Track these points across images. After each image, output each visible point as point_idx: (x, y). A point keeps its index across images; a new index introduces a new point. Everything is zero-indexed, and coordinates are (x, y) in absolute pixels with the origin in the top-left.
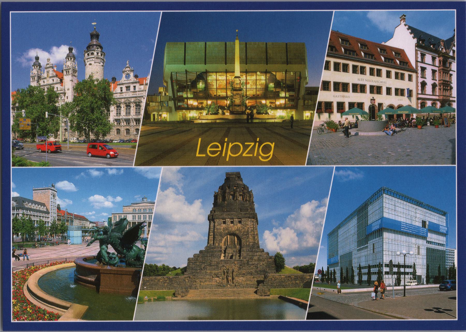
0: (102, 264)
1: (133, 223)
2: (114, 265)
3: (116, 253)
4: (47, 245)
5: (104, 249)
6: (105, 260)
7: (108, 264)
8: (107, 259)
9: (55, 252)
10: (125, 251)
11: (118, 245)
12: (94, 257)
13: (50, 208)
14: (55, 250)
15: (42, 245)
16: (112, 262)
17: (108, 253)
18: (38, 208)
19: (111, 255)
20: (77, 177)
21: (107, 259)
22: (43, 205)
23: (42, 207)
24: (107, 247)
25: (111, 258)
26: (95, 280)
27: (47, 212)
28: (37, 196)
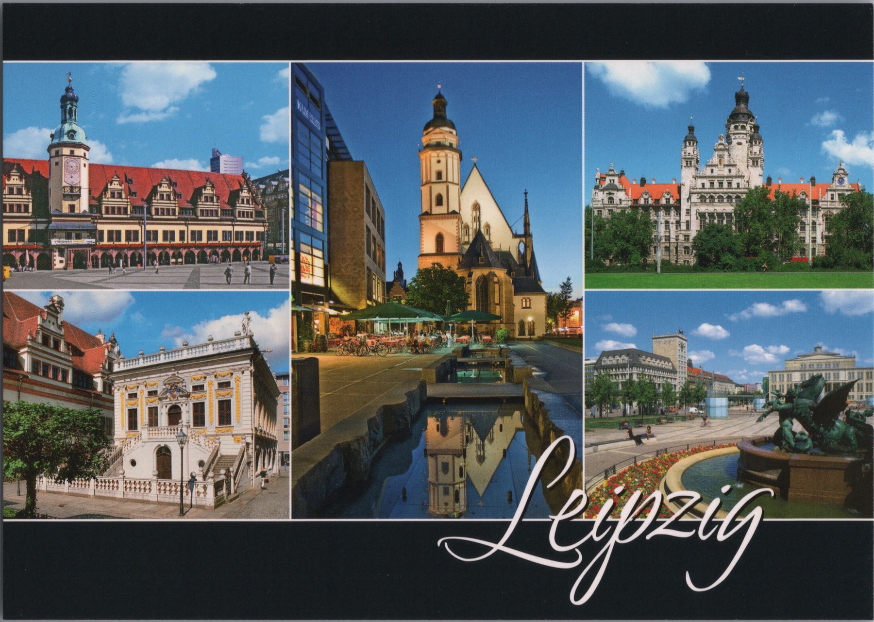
0: (783, 451)
2: (805, 452)
3: (807, 433)
4: (677, 419)
5: (787, 426)
6: (788, 443)
8: (793, 443)
9: (690, 430)
11: (810, 419)
12: (769, 438)
13: (676, 364)
14: (690, 427)
15: (670, 420)
16: (801, 447)
17: (794, 433)
18: (660, 365)
19: (798, 436)
20: (733, 318)
21: (793, 443)
24: (792, 423)
25: (797, 440)
27: (674, 371)
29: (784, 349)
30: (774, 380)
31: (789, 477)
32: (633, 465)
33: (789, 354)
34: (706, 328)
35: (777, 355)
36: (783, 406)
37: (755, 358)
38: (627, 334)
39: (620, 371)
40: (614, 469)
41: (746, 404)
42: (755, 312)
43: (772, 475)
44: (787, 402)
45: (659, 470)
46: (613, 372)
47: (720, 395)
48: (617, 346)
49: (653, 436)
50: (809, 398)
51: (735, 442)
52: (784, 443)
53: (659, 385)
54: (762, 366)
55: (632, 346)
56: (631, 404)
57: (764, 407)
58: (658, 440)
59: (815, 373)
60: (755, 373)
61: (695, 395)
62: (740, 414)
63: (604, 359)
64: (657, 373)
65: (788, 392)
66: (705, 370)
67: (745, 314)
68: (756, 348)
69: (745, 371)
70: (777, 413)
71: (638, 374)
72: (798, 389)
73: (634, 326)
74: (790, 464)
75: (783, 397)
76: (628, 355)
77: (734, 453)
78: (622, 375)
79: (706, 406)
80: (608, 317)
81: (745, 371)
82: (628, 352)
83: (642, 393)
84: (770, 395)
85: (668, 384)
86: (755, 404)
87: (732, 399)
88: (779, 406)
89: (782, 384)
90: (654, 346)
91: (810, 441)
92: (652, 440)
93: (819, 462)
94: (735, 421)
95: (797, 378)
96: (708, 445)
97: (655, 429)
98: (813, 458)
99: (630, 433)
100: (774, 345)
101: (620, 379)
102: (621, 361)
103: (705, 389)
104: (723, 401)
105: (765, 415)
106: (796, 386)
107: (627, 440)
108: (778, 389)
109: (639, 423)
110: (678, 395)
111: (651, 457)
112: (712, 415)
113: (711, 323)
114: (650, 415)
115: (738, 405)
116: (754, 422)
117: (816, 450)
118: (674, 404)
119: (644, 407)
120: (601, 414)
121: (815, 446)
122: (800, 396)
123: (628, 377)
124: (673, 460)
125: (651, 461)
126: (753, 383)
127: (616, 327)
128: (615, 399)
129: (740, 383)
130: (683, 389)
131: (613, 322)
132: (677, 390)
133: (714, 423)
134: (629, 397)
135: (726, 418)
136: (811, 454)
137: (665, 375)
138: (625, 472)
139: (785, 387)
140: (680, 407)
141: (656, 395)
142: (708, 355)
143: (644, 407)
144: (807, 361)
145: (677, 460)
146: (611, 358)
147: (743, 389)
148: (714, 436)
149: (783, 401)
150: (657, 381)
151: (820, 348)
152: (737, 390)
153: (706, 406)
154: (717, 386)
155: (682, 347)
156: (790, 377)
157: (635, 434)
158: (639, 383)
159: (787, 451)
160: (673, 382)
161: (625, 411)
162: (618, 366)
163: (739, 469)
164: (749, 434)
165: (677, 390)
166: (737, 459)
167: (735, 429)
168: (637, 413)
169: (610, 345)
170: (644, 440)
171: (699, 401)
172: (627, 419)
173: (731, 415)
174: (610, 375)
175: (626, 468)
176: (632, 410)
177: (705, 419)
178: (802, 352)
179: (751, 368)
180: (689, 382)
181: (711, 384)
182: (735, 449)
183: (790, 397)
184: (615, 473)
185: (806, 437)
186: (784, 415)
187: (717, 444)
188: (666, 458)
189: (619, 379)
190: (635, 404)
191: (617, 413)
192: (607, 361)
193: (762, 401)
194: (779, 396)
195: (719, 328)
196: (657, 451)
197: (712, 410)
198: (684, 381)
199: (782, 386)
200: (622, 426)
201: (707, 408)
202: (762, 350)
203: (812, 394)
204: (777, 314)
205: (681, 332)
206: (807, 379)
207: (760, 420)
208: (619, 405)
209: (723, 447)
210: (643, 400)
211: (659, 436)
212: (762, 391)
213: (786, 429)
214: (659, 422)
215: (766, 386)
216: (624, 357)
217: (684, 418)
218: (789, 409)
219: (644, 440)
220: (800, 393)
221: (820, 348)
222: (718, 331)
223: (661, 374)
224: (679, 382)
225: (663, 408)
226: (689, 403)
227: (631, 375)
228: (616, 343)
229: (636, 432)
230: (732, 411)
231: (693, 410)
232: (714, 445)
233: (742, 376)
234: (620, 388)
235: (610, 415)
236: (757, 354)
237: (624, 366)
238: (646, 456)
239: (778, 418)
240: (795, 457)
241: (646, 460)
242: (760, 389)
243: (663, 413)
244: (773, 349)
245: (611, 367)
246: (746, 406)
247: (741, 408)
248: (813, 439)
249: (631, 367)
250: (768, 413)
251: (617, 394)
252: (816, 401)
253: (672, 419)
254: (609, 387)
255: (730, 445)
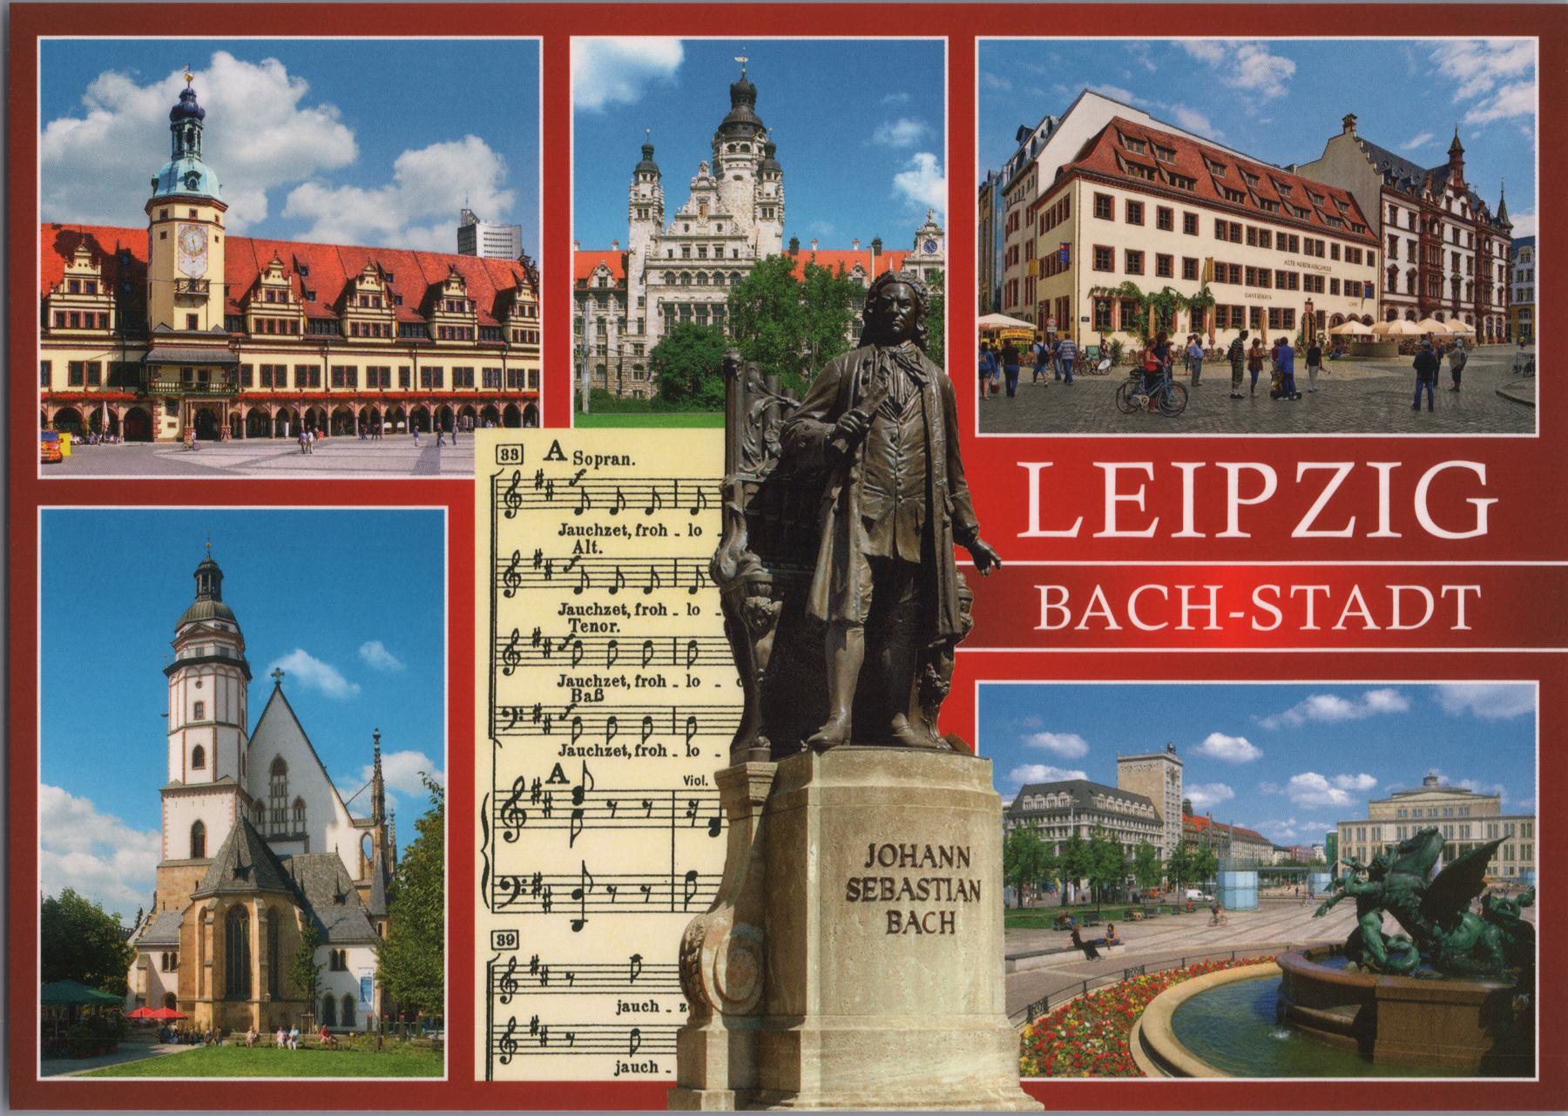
0: (1365, 969)
1: (1461, 847)
2: (1405, 972)
3: (1408, 936)
4: (1163, 912)
5: (1371, 924)
6: (1374, 955)
7: (1388, 970)
8: (1383, 956)
9: (1188, 933)
10: (1437, 930)
11: (1415, 912)
12: (1338, 946)
13: (1163, 810)
14: (1187, 926)
15: (1150, 913)
16: (1399, 963)
17: (1385, 938)
18: (1132, 811)
19: (1392, 942)
20: (1269, 724)
21: (1383, 956)
22: (1145, 801)
23: (1144, 807)
24: (1381, 919)
25: (1391, 951)
26: (1357, 1019)
27: (1158, 822)
28: (1129, 778)
29: (1366, 781)
30: (1348, 839)
31: (1375, 1019)
32: (1080, 997)
33: (1372, 790)
34: (1218, 743)
35: (1353, 793)
36: (1364, 887)
37: (1311, 797)
38: (1071, 754)
39: (1057, 822)
40: (1044, 1004)
41: (1295, 882)
42: (1312, 712)
43: (1344, 1016)
44: (1371, 879)
45: (1129, 1005)
46: (1044, 823)
47: (1245, 866)
48: (1052, 774)
49: (1117, 943)
50: (1412, 873)
51: (1274, 953)
52: (1366, 955)
53: (1130, 847)
54: (1324, 812)
55: (1080, 775)
56: (1077, 884)
57: (1328, 889)
58: (1128, 950)
59: (1425, 826)
60: (1312, 826)
61: (1198, 865)
62: (1282, 902)
63: (1027, 799)
64: (1125, 826)
65: (1374, 861)
66: (1215, 819)
67: (1292, 716)
68: (1313, 779)
69: (1292, 822)
70: (1353, 900)
71: (1090, 827)
72: (1393, 855)
73: (1082, 737)
74: (1378, 994)
75: (1364, 869)
76: (1071, 792)
77: (1271, 974)
78: (1060, 829)
79: (1218, 888)
80: (1032, 721)
81: (1292, 822)
82: (1071, 787)
83: (1098, 862)
84: (1341, 867)
85: (1147, 847)
86: (1312, 883)
87: (1266, 873)
88: (1356, 888)
89: (1365, 847)
90: (1122, 775)
91: (1414, 953)
92: (1116, 950)
93: (1433, 992)
94: (1274, 915)
95: (1390, 835)
96: (1221, 958)
97: (1121, 929)
98: (1418, 984)
99: (1076, 937)
100: (1347, 773)
101: (1057, 837)
102: (1058, 804)
103: (1216, 854)
104: (1248, 879)
105: (1330, 905)
106: (1388, 849)
107: (1069, 949)
108: (1354, 854)
109: (1092, 919)
110: (1164, 867)
111: (1113, 982)
112: (1228, 903)
113: (1228, 732)
114: (1112, 903)
115: (1278, 885)
116: (1310, 917)
117: (1426, 971)
118: (1158, 883)
119: (1100, 887)
120: (1020, 902)
121: (1424, 962)
122: (1396, 869)
123: (1071, 833)
124: (1155, 988)
125: (1114, 990)
126: (1308, 843)
127: (1049, 740)
128: (1047, 874)
129: (1280, 844)
130: (1175, 856)
131: (1041, 731)
132: (1164, 857)
133: (1232, 919)
134: (1073, 871)
135: (1254, 910)
136: (1418, 976)
137: (1141, 828)
138: (1065, 1010)
139: (1369, 850)
140: (1170, 889)
141: (1124, 867)
142: (1225, 791)
143: (1100, 887)
144: (1409, 804)
145: (1164, 987)
146: (1039, 798)
147: (1288, 856)
148: (1229, 943)
149: (1364, 877)
150: (1125, 840)
151: (1434, 779)
152: (1276, 858)
153: (1218, 888)
154: (1239, 851)
155: (1173, 776)
156: (1377, 834)
157: (1084, 939)
158: (1092, 844)
159: (1372, 971)
160: (1157, 843)
161: (1065, 895)
162: (1053, 813)
163: (1280, 1005)
164: (1301, 939)
165: (1164, 857)
166: (1276, 986)
167: (1274, 929)
168: (1089, 901)
169: (1038, 773)
170: (1102, 951)
171: (1204, 875)
172: (1070, 911)
173: (1264, 903)
174: (1037, 829)
175: (1069, 1002)
176: (1079, 895)
177: (1215, 912)
178: (1400, 786)
179: (1303, 815)
180: (1186, 843)
181: (1227, 846)
182: (1272, 967)
183: (1377, 870)
184: (1046, 1011)
185: (1406, 945)
186: (1366, 903)
187: (1239, 957)
188: (1141, 985)
189: (1054, 837)
190: (1084, 883)
191: (1052, 899)
192: (1031, 803)
193: (1325, 878)
194: (1356, 869)
195: (1242, 741)
196: (1126, 971)
197: (1228, 894)
198: (1177, 841)
199: (1362, 850)
200: (1060, 924)
201: (1220, 890)
202: (1325, 783)
203: (1418, 864)
204: (1352, 716)
205: (1170, 750)
206: (1410, 836)
207: (1320, 913)
208: (1055, 885)
209: (1249, 963)
210: (1100, 875)
211: (1129, 943)
212: (1324, 859)
213: (1370, 931)
214: (1129, 917)
215: (1331, 850)
216: (1063, 795)
217: (1176, 910)
218: (1375, 893)
219: (1102, 951)
220: (1395, 865)
221: (1434, 779)
222: (1240, 746)
223: (1133, 827)
224: (1166, 843)
225: (1137, 890)
226: (1185, 881)
227: (1077, 829)
228: (1049, 770)
229: (1087, 934)
230: (1268, 897)
231: (1193, 894)
232: (1232, 959)
233: (1285, 832)
234: (1057, 853)
235: (1038, 904)
236: (1315, 791)
237: (1063, 813)
238: (1105, 979)
239: (1354, 909)
240: (1385, 981)
241: (1108, 987)
242: (1321, 855)
243: (1136, 899)
244: (1345, 780)
245: (1039, 814)
246: (1293, 888)
247: (1284, 890)
248: (1422, 948)
249: (1078, 814)
250: (1337, 900)
251: (1051, 865)
252: (1426, 877)
253: (1152, 911)
254: (1036, 853)
255: (1261, 961)
